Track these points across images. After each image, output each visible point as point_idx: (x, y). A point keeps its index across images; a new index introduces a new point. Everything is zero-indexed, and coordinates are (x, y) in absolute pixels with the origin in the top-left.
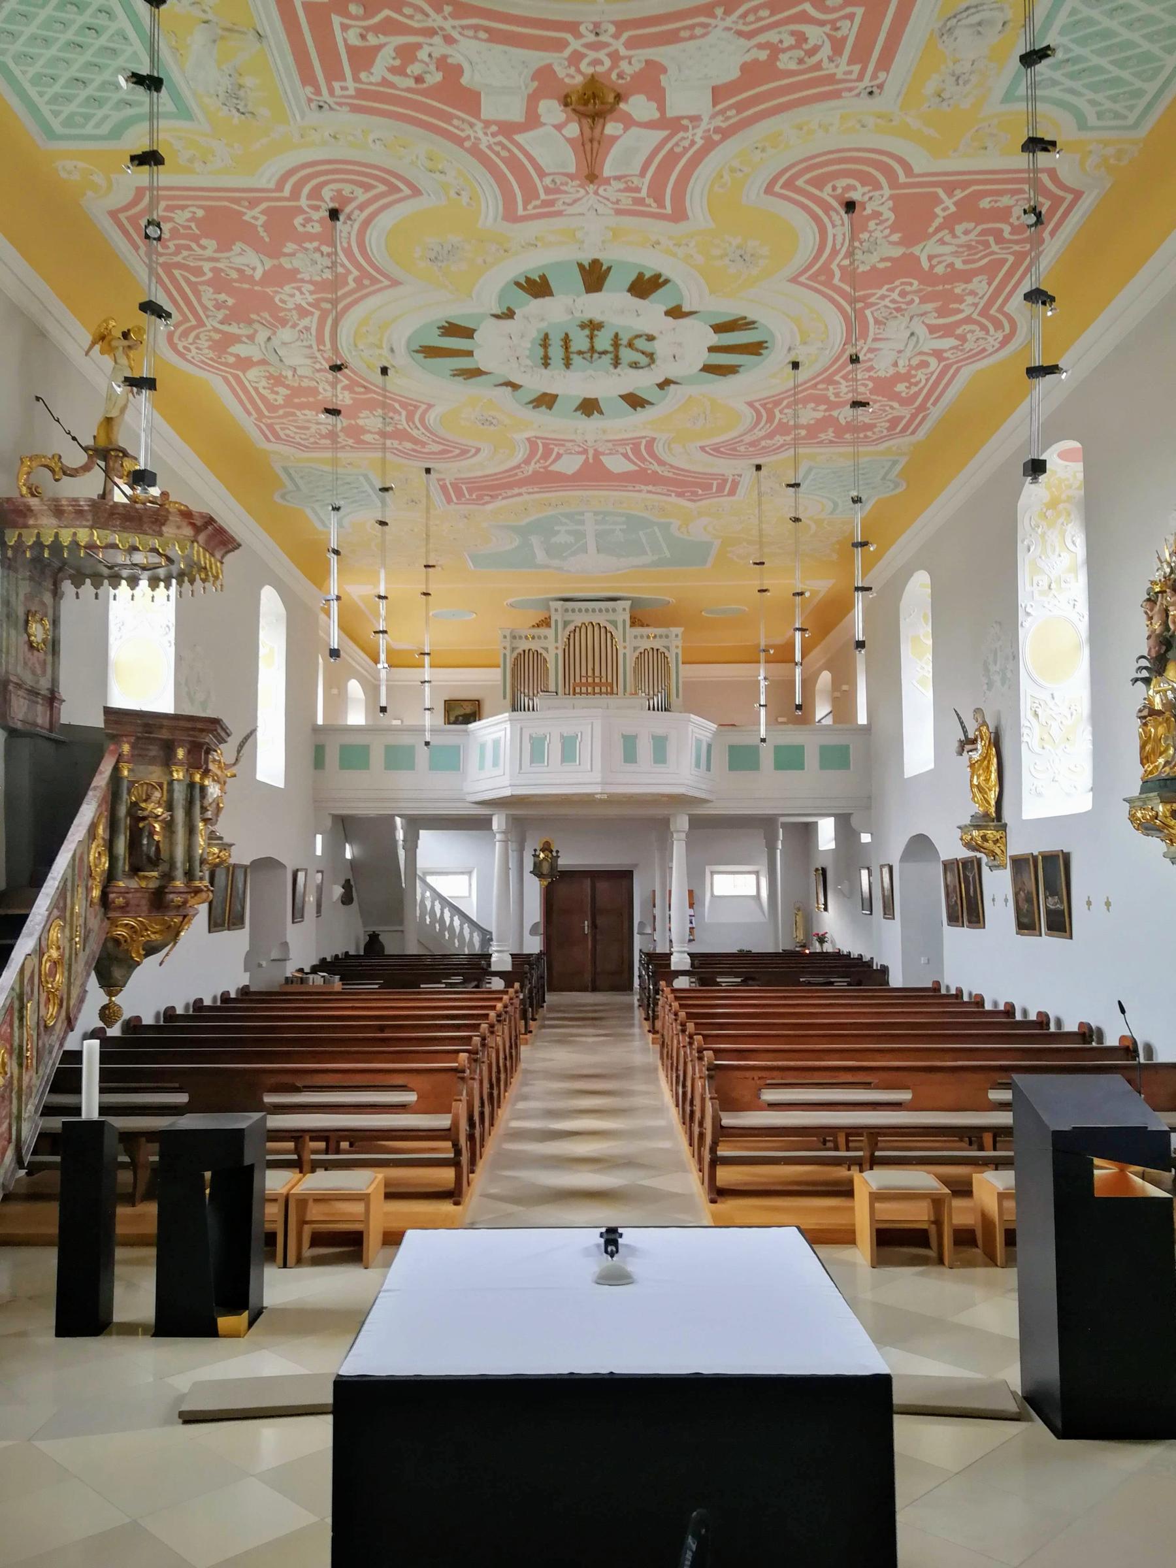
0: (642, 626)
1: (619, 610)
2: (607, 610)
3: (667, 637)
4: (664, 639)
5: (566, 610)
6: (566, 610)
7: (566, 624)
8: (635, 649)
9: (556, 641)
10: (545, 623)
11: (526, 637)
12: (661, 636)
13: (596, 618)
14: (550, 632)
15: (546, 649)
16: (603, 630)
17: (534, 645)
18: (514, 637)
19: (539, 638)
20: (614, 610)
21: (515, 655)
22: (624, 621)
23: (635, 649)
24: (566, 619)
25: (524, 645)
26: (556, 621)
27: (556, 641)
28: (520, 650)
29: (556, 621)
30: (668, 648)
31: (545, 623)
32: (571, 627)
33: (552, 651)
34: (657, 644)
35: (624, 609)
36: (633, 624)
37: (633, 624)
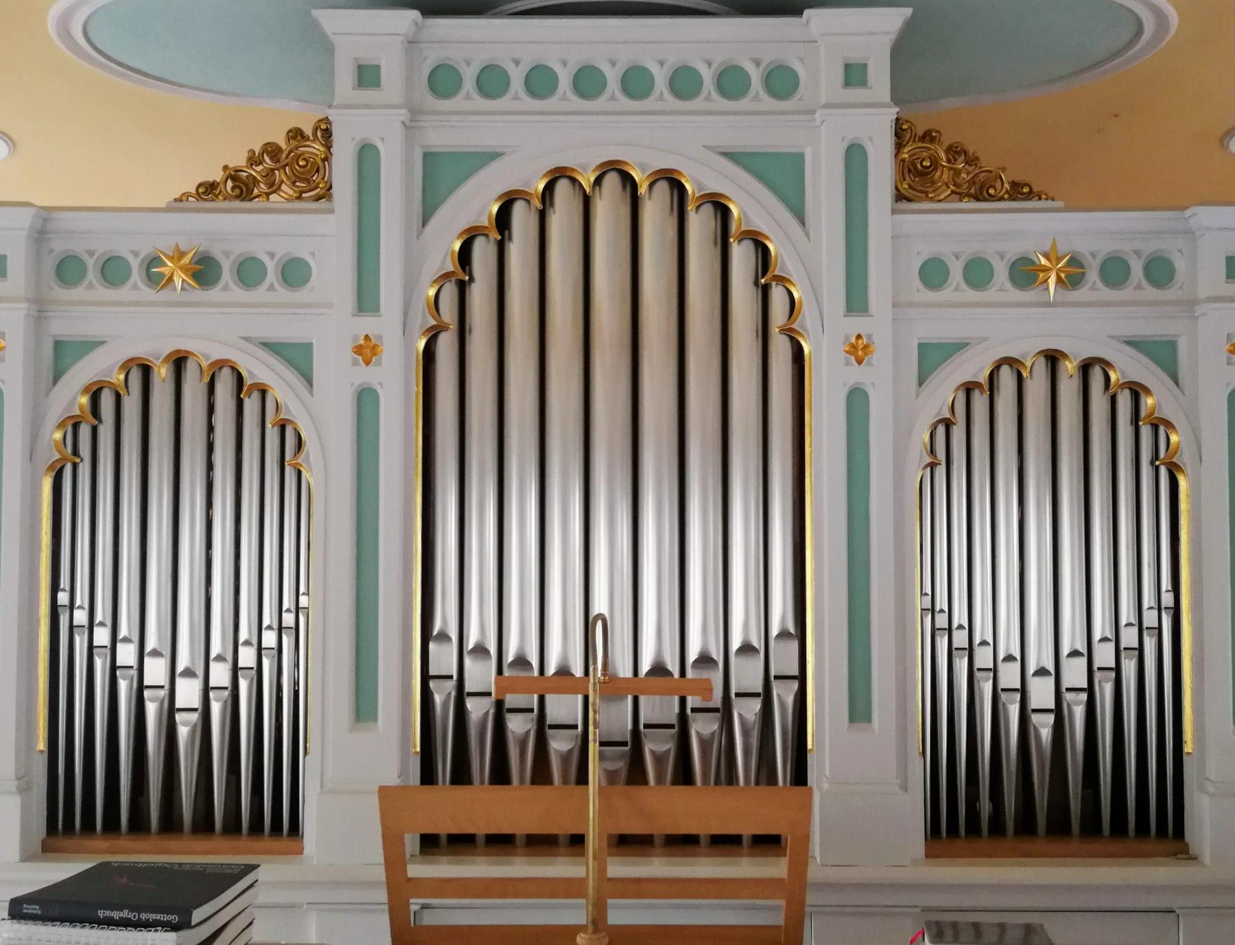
0: (980, 191)
1: (820, 79)
2: (731, 82)
3: (1159, 271)
4: (1138, 287)
5: (443, 81)
6: (443, 81)
7: (438, 175)
8: (931, 358)
9: (366, 300)
10: (292, 168)
11: (154, 276)
12: (1114, 271)
13: (650, 140)
14: (318, 235)
15: (297, 358)
16: (700, 224)
17: (213, 328)
18: (68, 270)
19: (249, 272)
20: (781, 82)
21: (70, 396)
22: (855, 157)
23: (931, 358)
24: (441, 137)
25: (135, 327)
26: (367, 155)
27: (366, 300)
28: (102, 365)
29: (367, 155)
30: (1163, 354)
31: (292, 168)
32: (475, 202)
33: (337, 376)
34: (1083, 327)
35: (854, 75)
36: (917, 180)
37: (917, 180)
